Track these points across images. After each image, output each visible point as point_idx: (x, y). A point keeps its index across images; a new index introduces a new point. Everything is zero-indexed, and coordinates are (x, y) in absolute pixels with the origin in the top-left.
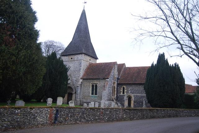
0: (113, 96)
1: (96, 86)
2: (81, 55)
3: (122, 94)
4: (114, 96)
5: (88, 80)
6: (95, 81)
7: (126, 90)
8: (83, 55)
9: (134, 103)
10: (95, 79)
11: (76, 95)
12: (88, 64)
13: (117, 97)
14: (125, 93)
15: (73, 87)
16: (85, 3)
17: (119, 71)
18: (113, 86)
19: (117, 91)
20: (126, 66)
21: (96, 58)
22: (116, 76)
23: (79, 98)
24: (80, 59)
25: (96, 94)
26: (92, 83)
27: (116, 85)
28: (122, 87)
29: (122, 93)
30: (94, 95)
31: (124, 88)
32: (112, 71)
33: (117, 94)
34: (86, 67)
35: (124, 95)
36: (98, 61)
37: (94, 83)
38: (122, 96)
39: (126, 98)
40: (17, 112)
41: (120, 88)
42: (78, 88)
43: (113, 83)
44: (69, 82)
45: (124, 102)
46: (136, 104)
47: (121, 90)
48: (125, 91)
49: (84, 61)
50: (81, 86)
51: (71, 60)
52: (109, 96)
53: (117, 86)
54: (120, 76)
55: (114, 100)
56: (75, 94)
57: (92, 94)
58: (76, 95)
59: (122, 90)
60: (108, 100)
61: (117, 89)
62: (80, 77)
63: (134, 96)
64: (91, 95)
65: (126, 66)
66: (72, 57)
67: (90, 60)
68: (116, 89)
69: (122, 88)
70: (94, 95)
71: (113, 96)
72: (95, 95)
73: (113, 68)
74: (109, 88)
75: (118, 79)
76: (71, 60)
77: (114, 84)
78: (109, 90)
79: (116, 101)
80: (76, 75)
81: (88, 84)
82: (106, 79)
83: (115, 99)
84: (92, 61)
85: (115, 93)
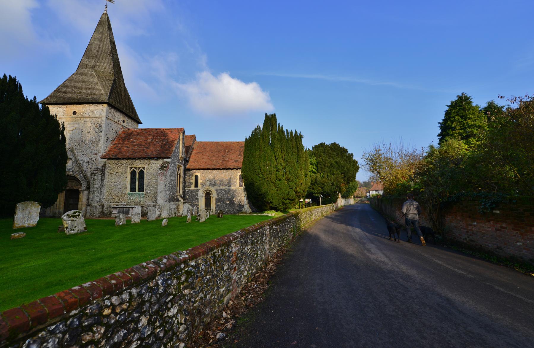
0: (177, 192)
1: (142, 173)
3: (193, 187)
4: (179, 192)
5: (122, 161)
6: (139, 162)
9: (216, 202)
10: (139, 159)
11: (88, 195)
12: (119, 129)
13: (184, 192)
14: (200, 186)
15: (80, 177)
19: (185, 183)
21: (138, 122)
24: (98, 116)
25: (141, 189)
26: (131, 168)
29: (193, 186)
30: (137, 192)
35: (198, 190)
36: (140, 126)
37: (136, 168)
38: (194, 191)
39: (201, 195)
42: (96, 178)
43: (177, 167)
44: (69, 165)
45: (198, 201)
46: (221, 204)
47: (191, 181)
49: (109, 121)
50: (103, 175)
52: (171, 191)
53: (185, 174)
55: (180, 199)
56: (86, 193)
57: (133, 189)
58: (88, 195)
59: (193, 181)
60: (169, 199)
61: (184, 179)
62: (100, 154)
63: (216, 190)
66: (75, 108)
67: (124, 122)
68: (182, 180)
69: (194, 178)
70: (137, 192)
71: (177, 192)
72: (139, 191)
74: (171, 176)
77: (179, 171)
78: (172, 180)
80: (89, 151)
81: (122, 169)
84: (129, 125)
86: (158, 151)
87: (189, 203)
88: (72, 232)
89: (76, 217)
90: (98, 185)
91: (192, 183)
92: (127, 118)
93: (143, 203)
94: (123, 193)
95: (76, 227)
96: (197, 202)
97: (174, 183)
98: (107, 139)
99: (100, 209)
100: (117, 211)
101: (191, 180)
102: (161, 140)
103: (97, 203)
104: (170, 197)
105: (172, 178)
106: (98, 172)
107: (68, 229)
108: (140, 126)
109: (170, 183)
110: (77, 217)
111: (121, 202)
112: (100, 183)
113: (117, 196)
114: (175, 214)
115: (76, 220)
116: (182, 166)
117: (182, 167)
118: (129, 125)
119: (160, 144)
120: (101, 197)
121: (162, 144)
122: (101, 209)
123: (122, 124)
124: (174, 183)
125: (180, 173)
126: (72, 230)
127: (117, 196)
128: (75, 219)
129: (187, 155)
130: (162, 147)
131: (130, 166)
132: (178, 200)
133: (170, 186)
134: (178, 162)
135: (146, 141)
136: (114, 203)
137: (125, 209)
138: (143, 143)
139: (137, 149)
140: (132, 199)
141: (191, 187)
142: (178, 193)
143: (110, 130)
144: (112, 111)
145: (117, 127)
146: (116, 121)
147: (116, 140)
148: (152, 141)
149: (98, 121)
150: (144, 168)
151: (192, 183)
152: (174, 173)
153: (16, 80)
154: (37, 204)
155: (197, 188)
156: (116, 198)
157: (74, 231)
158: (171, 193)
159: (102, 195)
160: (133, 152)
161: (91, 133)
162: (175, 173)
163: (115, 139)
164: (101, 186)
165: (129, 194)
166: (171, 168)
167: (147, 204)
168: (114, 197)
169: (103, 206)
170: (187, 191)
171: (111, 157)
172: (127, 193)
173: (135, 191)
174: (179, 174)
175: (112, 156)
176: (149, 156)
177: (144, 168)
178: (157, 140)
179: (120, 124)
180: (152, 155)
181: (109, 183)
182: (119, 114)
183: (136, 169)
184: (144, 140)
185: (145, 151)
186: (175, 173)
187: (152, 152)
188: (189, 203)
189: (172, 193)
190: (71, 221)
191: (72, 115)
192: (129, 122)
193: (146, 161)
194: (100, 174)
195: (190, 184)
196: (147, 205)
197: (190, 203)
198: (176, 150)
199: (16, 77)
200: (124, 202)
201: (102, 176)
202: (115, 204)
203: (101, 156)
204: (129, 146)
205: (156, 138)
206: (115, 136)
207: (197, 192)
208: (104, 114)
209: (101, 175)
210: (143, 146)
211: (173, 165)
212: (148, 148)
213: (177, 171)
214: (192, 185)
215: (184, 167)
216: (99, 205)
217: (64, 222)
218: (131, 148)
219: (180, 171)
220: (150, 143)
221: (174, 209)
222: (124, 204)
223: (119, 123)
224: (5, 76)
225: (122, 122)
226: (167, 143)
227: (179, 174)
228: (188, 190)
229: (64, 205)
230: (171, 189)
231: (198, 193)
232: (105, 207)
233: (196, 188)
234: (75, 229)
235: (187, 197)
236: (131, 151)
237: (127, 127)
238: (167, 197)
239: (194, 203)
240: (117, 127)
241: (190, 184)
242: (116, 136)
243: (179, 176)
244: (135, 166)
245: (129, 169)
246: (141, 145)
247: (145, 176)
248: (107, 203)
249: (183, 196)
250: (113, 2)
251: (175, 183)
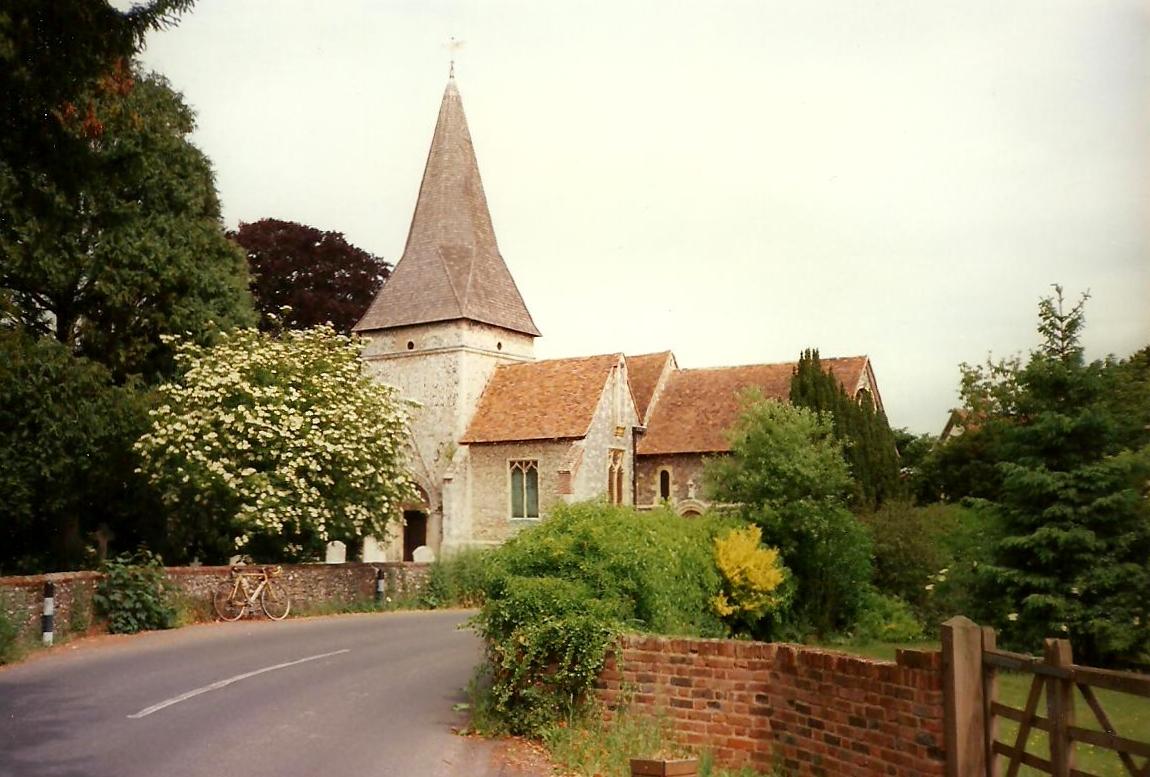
2: (452, 329)
6: (526, 449)
7: (674, 483)
8: (464, 326)
11: (441, 523)
12: (489, 367)
17: (641, 392)
18: (611, 469)
20: (681, 367)
22: (630, 420)
23: (455, 532)
26: (512, 463)
27: (626, 463)
28: (655, 472)
31: (665, 476)
32: (604, 398)
34: (484, 382)
36: (539, 351)
37: (521, 463)
40: (291, 578)
41: (647, 474)
47: (653, 488)
48: (673, 488)
54: (649, 414)
56: (436, 517)
59: (657, 487)
64: (509, 517)
69: (658, 478)
73: (607, 386)
74: (589, 479)
75: (637, 433)
77: (615, 463)
84: (515, 348)
91: (654, 492)
101: (652, 484)
129: (643, 415)
131: (512, 459)
134: (612, 443)
141: (652, 503)
147: (484, 395)
150: (535, 463)
151: (654, 492)
161: (440, 388)
165: (512, 522)
166: (588, 460)
173: (523, 517)
177: (535, 463)
193: (540, 447)
211: (593, 452)
219: (619, 461)
243: (616, 476)
244: (520, 459)
245: (508, 464)
247: (539, 481)
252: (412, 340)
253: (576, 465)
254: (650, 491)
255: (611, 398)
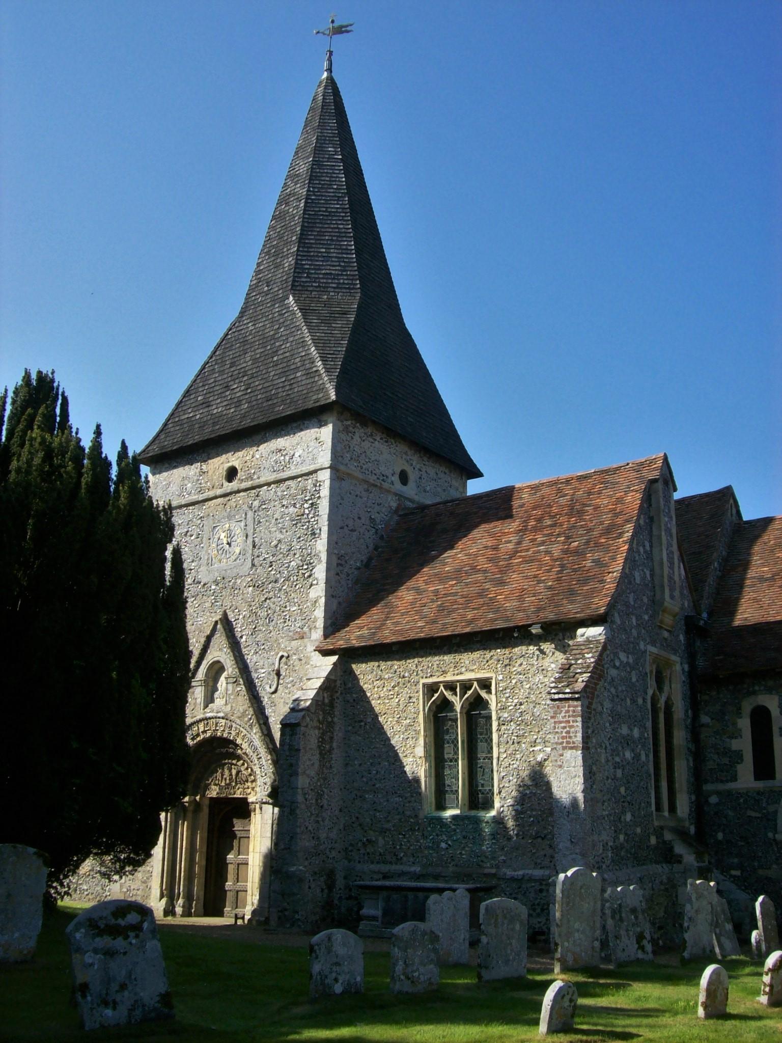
0: (659, 808)
4: (672, 808)
16: (340, 30)
19: (698, 755)
20: (745, 518)
24: (305, 469)
28: (739, 713)
33: (698, 778)
36: (474, 487)
37: (451, 687)
47: (735, 745)
51: (229, 487)
53: (694, 704)
59: (744, 744)
60: (616, 849)
61: (695, 731)
65: (745, 518)
67: (404, 478)
68: (680, 737)
69: (745, 724)
71: (659, 808)
74: (616, 718)
76: (234, 485)
77: (660, 688)
78: (627, 741)
79: (699, 856)
82: (580, 631)
83: (682, 834)
85: (682, 769)
86: (550, 588)
87: (733, 872)
88: (109, 1012)
89: (126, 937)
90: (308, 776)
91: (738, 756)
92: (415, 459)
93: (493, 871)
94: (408, 813)
95: (123, 987)
96: (775, 866)
97: (637, 757)
98: (338, 565)
99: (318, 890)
100: (381, 904)
102: (559, 535)
103: (306, 863)
104: (622, 837)
105: (625, 730)
106: (304, 717)
107: (89, 998)
108: (474, 487)
109: (617, 759)
110: (132, 934)
111: (399, 860)
112: (317, 765)
113: (383, 832)
114: (638, 942)
115: (125, 953)
116: (677, 659)
117: (678, 667)
118: (428, 488)
119: (556, 550)
120: (323, 835)
121: (565, 552)
122: (322, 890)
123: (398, 486)
124: (637, 757)
125: (669, 699)
126: (106, 1004)
127: (383, 832)
128: (119, 943)
130: (563, 566)
132: (667, 855)
133: (619, 773)
134: (653, 643)
135: (495, 548)
136: (373, 867)
137: (411, 895)
138: (482, 562)
139: (455, 594)
140: (443, 845)
142: (666, 814)
143: (350, 523)
144: (357, 437)
145: (379, 504)
146: (372, 479)
148: (519, 543)
149: (304, 490)
151: (738, 756)
152: (634, 701)
153: (53, 381)
154: (34, 857)
155: (769, 783)
156: (381, 841)
157: (114, 1008)
158: (624, 812)
159: (327, 822)
160: (441, 609)
162: (640, 701)
163: (370, 559)
164: (318, 780)
166: (613, 672)
167: (509, 873)
168: (372, 835)
169: (331, 875)
170: (714, 799)
171: (354, 642)
172: (421, 815)
174: (661, 704)
175: (359, 637)
176: (507, 619)
177: (485, 684)
178: (540, 538)
179: (388, 491)
180: (521, 615)
181: (350, 769)
182: (384, 448)
183: (456, 695)
184: (486, 547)
185: (491, 599)
186: (640, 701)
187: (521, 598)
188: (733, 872)
189: (628, 817)
190: (105, 954)
191: (226, 484)
192: (424, 475)
194: (316, 724)
195: (725, 760)
196: (513, 879)
197: (737, 873)
198: (637, 574)
199: (53, 373)
200: (412, 859)
201: (323, 734)
202: (373, 867)
203: (317, 644)
204: (422, 586)
205: (535, 529)
206: (371, 546)
207: (771, 809)
208: (325, 458)
209: (317, 732)
210: (480, 576)
211: (623, 656)
212: (501, 583)
213: (650, 692)
214: (739, 767)
215: (686, 667)
216: (315, 873)
217: (76, 958)
218: (433, 592)
219: (666, 688)
220: (510, 558)
221: (634, 911)
222: (413, 869)
223: (386, 485)
224: (27, 377)
225: (396, 479)
226: (588, 542)
227: (661, 704)
228: (718, 793)
229: (204, 863)
230: (622, 790)
231: (776, 812)
232: (340, 882)
233: (760, 785)
234: (118, 998)
235: (720, 836)
236: (430, 610)
237: (416, 498)
238: (604, 837)
239: (760, 872)
240: (379, 504)
241: (725, 760)
242: (376, 548)
244: (449, 678)
246: (474, 569)
248: (346, 862)
249: (692, 830)
250: (348, 29)
251: (643, 758)
252: (236, 464)
253: (487, 757)
254: (727, 752)
255: (648, 548)
